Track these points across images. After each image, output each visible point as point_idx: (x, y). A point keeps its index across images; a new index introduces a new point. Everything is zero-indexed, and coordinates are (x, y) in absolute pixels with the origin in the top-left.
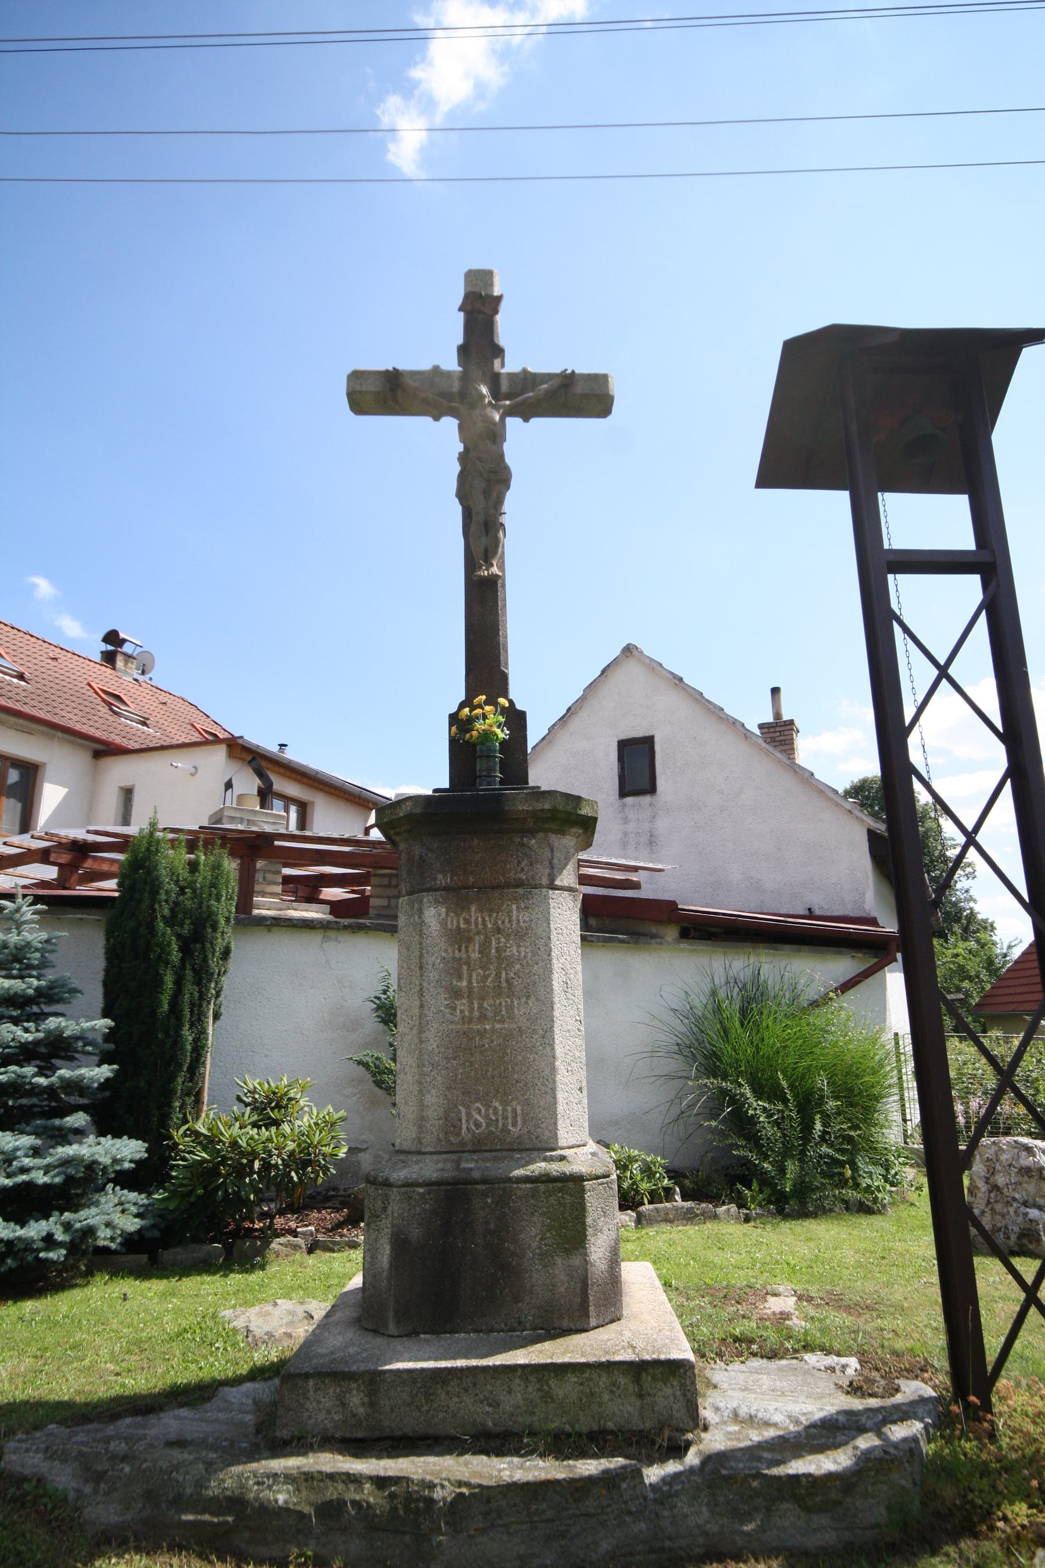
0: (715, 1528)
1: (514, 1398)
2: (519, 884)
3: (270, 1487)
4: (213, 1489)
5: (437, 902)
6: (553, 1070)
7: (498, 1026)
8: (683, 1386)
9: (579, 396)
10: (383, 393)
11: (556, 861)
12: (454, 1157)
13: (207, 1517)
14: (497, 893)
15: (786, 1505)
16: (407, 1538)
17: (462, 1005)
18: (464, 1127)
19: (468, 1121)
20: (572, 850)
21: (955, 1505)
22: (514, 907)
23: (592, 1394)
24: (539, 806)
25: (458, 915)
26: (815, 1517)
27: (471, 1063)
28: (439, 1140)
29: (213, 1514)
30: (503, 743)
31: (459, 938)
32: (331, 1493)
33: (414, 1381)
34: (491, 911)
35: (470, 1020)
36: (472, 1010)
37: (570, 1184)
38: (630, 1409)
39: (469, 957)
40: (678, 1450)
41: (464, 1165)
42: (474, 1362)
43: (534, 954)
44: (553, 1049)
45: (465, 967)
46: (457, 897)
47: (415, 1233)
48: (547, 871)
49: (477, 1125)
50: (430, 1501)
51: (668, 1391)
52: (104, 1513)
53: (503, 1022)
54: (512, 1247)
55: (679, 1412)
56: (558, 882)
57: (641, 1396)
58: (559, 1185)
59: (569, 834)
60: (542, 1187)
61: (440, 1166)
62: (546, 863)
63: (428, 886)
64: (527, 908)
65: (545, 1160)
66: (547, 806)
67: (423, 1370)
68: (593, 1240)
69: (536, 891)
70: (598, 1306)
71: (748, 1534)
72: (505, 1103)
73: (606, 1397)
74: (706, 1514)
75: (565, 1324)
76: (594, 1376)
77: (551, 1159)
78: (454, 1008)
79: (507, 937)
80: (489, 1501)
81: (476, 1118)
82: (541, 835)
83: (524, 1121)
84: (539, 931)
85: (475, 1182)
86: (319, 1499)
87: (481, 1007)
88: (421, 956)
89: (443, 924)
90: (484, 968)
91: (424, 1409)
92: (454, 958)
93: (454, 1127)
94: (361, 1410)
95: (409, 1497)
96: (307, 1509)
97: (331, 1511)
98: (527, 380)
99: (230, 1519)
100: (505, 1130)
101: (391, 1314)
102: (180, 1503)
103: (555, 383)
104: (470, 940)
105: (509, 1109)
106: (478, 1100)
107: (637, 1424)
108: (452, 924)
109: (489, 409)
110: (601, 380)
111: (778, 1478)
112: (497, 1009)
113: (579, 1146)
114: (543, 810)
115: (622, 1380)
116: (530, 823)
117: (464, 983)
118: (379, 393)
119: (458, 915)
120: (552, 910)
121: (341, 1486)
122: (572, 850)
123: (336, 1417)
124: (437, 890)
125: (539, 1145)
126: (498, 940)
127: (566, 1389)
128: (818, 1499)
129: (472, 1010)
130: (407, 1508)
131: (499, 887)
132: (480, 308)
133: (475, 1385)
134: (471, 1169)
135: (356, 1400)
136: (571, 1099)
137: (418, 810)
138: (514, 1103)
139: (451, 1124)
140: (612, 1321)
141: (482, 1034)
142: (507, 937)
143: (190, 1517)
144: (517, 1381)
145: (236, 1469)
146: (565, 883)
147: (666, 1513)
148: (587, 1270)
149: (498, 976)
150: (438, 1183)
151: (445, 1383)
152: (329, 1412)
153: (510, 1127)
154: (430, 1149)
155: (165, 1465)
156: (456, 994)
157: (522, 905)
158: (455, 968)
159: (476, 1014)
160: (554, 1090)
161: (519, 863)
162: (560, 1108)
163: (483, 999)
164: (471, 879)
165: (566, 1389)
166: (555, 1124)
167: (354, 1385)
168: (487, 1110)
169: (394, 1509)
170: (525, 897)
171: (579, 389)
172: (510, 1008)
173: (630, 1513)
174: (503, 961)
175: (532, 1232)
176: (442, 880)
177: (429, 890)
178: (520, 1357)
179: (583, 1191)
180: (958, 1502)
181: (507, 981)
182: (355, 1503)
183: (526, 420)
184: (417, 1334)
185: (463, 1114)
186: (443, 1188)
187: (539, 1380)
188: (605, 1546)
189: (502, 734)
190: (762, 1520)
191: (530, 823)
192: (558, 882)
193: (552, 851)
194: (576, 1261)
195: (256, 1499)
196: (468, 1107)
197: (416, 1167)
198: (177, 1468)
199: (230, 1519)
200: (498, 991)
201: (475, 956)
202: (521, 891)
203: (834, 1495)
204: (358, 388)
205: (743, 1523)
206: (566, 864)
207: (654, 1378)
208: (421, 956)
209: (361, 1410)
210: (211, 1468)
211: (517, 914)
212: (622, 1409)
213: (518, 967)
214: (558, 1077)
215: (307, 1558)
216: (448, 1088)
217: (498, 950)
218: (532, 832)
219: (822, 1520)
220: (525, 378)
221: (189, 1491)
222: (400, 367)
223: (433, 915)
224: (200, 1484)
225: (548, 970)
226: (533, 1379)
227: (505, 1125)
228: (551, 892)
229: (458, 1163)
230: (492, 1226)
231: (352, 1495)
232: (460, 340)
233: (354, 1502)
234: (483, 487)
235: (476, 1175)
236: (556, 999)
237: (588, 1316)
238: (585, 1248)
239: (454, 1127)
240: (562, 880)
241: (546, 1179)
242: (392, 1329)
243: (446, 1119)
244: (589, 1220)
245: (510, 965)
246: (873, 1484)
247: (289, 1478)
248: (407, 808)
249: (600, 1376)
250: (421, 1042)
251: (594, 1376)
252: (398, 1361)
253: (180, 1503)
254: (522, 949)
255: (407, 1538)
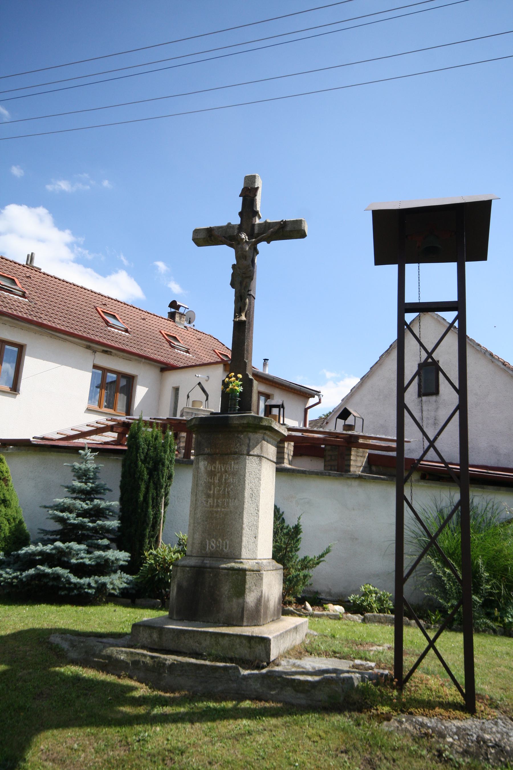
0: (261, 691)
1: (207, 642)
2: (235, 453)
3: (120, 654)
4: (104, 653)
5: (204, 459)
6: (242, 528)
7: (223, 510)
8: (265, 646)
9: (289, 231)
10: (207, 237)
11: (251, 444)
12: (202, 558)
13: (101, 660)
14: (227, 457)
15: (289, 688)
16: (156, 674)
17: (210, 500)
18: (208, 547)
19: (209, 546)
20: (260, 440)
21: (358, 702)
22: (233, 462)
23: (233, 645)
24: (242, 422)
25: (211, 465)
26: (299, 695)
27: (212, 523)
28: (198, 551)
29: (102, 659)
30: (241, 392)
31: (211, 474)
32: (137, 658)
33: (174, 632)
34: (224, 464)
35: (213, 507)
36: (213, 504)
37: (241, 572)
38: (246, 651)
39: (214, 482)
40: (259, 667)
41: (205, 562)
42: (195, 629)
43: (239, 482)
44: (242, 520)
45: (213, 486)
46: (212, 458)
47: (185, 584)
48: (247, 448)
49: (212, 547)
50: (165, 664)
51: (260, 647)
52: (73, 655)
53: (225, 508)
54: (218, 593)
55: (263, 655)
56: (251, 453)
57: (250, 648)
58: (237, 572)
59: (259, 433)
60: (231, 572)
61: (197, 561)
62: (246, 445)
63: (201, 453)
64: (237, 463)
65: (235, 562)
66: (245, 422)
67: (177, 629)
68: (248, 594)
69: (242, 456)
70: (247, 618)
71: (272, 695)
72: (223, 540)
73: (238, 646)
74: (259, 685)
75: (235, 623)
76: (235, 639)
77: (237, 562)
78: (207, 502)
79: (229, 475)
80: (183, 666)
81: (212, 545)
82: (245, 433)
83: (229, 547)
84: (241, 473)
85: (206, 568)
86: (133, 659)
87: (217, 502)
88: (197, 481)
89: (206, 468)
90: (219, 486)
91: (177, 642)
92: (209, 482)
93: (204, 547)
94: (156, 640)
95: (159, 662)
96: (129, 661)
97: (135, 663)
98: (267, 225)
99: (107, 661)
100: (222, 550)
101: (175, 612)
102: (94, 655)
103: (276, 228)
104: (215, 475)
105: (224, 542)
106: (213, 538)
107: (248, 657)
108: (209, 469)
109: (245, 244)
110: (299, 223)
111: (288, 679)
112: (223, 503)
113: (252, 559)
114: (244, 423)
115: (244, 641)
116: (240, 428)
117: (212, 492)
118: (204, 238)
119: (211, 465)
120: (247, 464)
121: (140, 657)
122: (260, 440)
123: (149, 641)
124: (205, 454)
125: (234, 557)
126: (226, 475)
127: (225, 642)
128: (301, 688)
129: (213, 504)
130: (157, 665)
131: (227, 454)
132: (249, 194)
133: (194, 636)
134: (207, 563)
135: (155, 636)
136: (250, 540)
137: (197, 423)
138: (226, 540)
139: (203, 546)
140: (255, 626)
141: (217, 512)
142: (229, 475)
143: (96, 660)
144: (208, 637)
145: (111, 648)
146: (255, 453)
147: (245, 683)
148: (244, 605)
149: (224, 490)
150: (194, 567)
151: (184, 634)
152: (146, 638)
153: (224, 549)
154: (194, 555)
155: (92, 644)
156: (208, 496)
157: (236, 462)
158: (209, 486)
159: (215, 504)
160: (241, 536)
161: (236, 444)
162: (244, 544)
163: (218, 499)
164: (217, 451)
165: (225, 642)
166: (241, 549)
167: (155, 631)
168: (216, 542)
169: (154, 665)
170: (237, 459)
171: (288, 228)
172: (228, 503)
173: (231, 680)
174: (227, 484)
175: (226, 589)
176: (207, 451)
177: (202, 454)
178: (211, 630)
179: (245, 575)
180: (360, 701)
181: (228, 492)
182: (143, 662)
183: (268, 243)
184: (183, 620)
185: (208, 543)
186: (196, 569)
187: (215, 637)
188: (220, 688)
189: (240, 389)
190: (278, 691)
191: (240, 428)
192: (251, 453)
193: (249, 440)
194: (241, 601)
195: (115, 657)
196: (209, 540)
197: (188, 561)
198: (95, 646)
199: (107, 661)
200: (224, 496)
201: (217, 481)
202: (236, 456)
203: (307, 688)
204: (196, 237)
205: (271, 690)
206: (257, 445)
207: (255, 642)
208: (197, 481)
209: (156, 640)
210: (105, 647)
211: (234, 466)
212: (243, 651)
213: (232, 486)
214: (244, 531)
215: (126, 675)
216: (203, 532)
217: (225, 479)
218: (242, 432)
219: (302, 696)
220: (265, 225)
221: (97, 652)
222: (212, 226)
223: (202, 465)
224: (101, 651)
225: (243, 489)
226: (213, 637)
227: (222, 548)
228: (247, 457)
229: (203, 561)
230: (212, 585)
231: (143, 659)
232: (240, 210)
233: (143, 662)
234: (242, 280)
235: (208, 565)
236: (246, 500)
237: (243, 621)
238: (244, 596)
239: (204, 547)
240: (254, 452)
241: (232, 569)
242: (175, 617)
243: (201, 544)
244: (247, 586)
245: (229, 486)
246: (324, 687)
247: (126, 653)
248: (193, 423)
249: (236, 639)
250: (195, 514)
251: (235, 639)
252: (171, 625)
253: (94, 655)
254: (234, 480)
255: (156, 674)
